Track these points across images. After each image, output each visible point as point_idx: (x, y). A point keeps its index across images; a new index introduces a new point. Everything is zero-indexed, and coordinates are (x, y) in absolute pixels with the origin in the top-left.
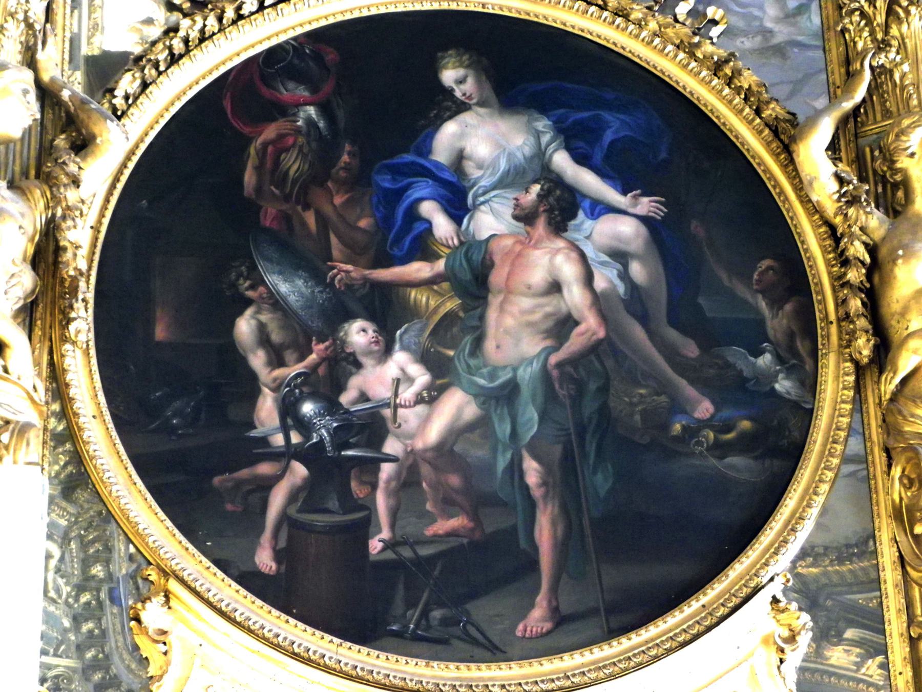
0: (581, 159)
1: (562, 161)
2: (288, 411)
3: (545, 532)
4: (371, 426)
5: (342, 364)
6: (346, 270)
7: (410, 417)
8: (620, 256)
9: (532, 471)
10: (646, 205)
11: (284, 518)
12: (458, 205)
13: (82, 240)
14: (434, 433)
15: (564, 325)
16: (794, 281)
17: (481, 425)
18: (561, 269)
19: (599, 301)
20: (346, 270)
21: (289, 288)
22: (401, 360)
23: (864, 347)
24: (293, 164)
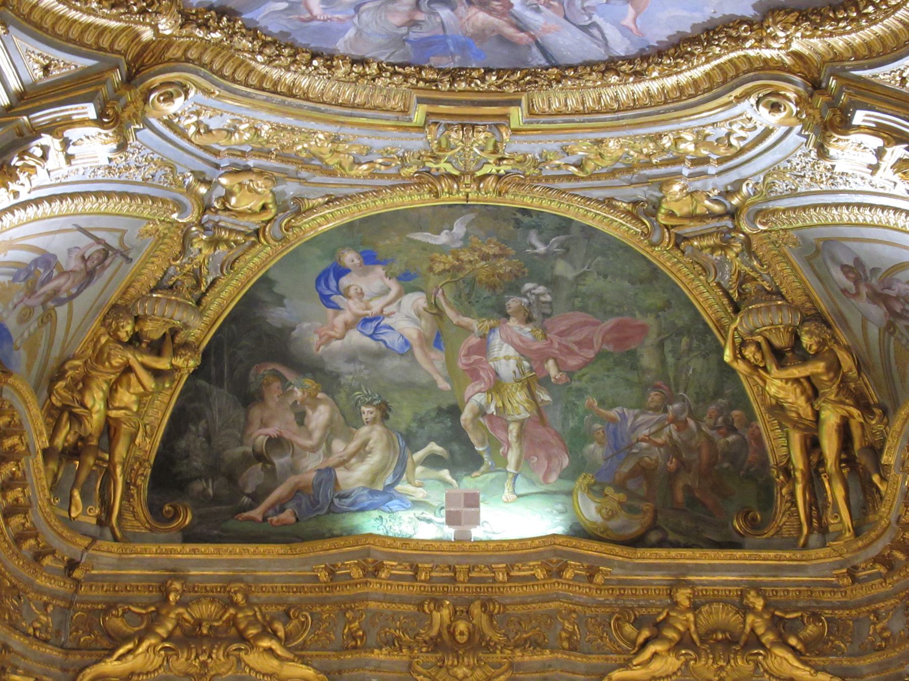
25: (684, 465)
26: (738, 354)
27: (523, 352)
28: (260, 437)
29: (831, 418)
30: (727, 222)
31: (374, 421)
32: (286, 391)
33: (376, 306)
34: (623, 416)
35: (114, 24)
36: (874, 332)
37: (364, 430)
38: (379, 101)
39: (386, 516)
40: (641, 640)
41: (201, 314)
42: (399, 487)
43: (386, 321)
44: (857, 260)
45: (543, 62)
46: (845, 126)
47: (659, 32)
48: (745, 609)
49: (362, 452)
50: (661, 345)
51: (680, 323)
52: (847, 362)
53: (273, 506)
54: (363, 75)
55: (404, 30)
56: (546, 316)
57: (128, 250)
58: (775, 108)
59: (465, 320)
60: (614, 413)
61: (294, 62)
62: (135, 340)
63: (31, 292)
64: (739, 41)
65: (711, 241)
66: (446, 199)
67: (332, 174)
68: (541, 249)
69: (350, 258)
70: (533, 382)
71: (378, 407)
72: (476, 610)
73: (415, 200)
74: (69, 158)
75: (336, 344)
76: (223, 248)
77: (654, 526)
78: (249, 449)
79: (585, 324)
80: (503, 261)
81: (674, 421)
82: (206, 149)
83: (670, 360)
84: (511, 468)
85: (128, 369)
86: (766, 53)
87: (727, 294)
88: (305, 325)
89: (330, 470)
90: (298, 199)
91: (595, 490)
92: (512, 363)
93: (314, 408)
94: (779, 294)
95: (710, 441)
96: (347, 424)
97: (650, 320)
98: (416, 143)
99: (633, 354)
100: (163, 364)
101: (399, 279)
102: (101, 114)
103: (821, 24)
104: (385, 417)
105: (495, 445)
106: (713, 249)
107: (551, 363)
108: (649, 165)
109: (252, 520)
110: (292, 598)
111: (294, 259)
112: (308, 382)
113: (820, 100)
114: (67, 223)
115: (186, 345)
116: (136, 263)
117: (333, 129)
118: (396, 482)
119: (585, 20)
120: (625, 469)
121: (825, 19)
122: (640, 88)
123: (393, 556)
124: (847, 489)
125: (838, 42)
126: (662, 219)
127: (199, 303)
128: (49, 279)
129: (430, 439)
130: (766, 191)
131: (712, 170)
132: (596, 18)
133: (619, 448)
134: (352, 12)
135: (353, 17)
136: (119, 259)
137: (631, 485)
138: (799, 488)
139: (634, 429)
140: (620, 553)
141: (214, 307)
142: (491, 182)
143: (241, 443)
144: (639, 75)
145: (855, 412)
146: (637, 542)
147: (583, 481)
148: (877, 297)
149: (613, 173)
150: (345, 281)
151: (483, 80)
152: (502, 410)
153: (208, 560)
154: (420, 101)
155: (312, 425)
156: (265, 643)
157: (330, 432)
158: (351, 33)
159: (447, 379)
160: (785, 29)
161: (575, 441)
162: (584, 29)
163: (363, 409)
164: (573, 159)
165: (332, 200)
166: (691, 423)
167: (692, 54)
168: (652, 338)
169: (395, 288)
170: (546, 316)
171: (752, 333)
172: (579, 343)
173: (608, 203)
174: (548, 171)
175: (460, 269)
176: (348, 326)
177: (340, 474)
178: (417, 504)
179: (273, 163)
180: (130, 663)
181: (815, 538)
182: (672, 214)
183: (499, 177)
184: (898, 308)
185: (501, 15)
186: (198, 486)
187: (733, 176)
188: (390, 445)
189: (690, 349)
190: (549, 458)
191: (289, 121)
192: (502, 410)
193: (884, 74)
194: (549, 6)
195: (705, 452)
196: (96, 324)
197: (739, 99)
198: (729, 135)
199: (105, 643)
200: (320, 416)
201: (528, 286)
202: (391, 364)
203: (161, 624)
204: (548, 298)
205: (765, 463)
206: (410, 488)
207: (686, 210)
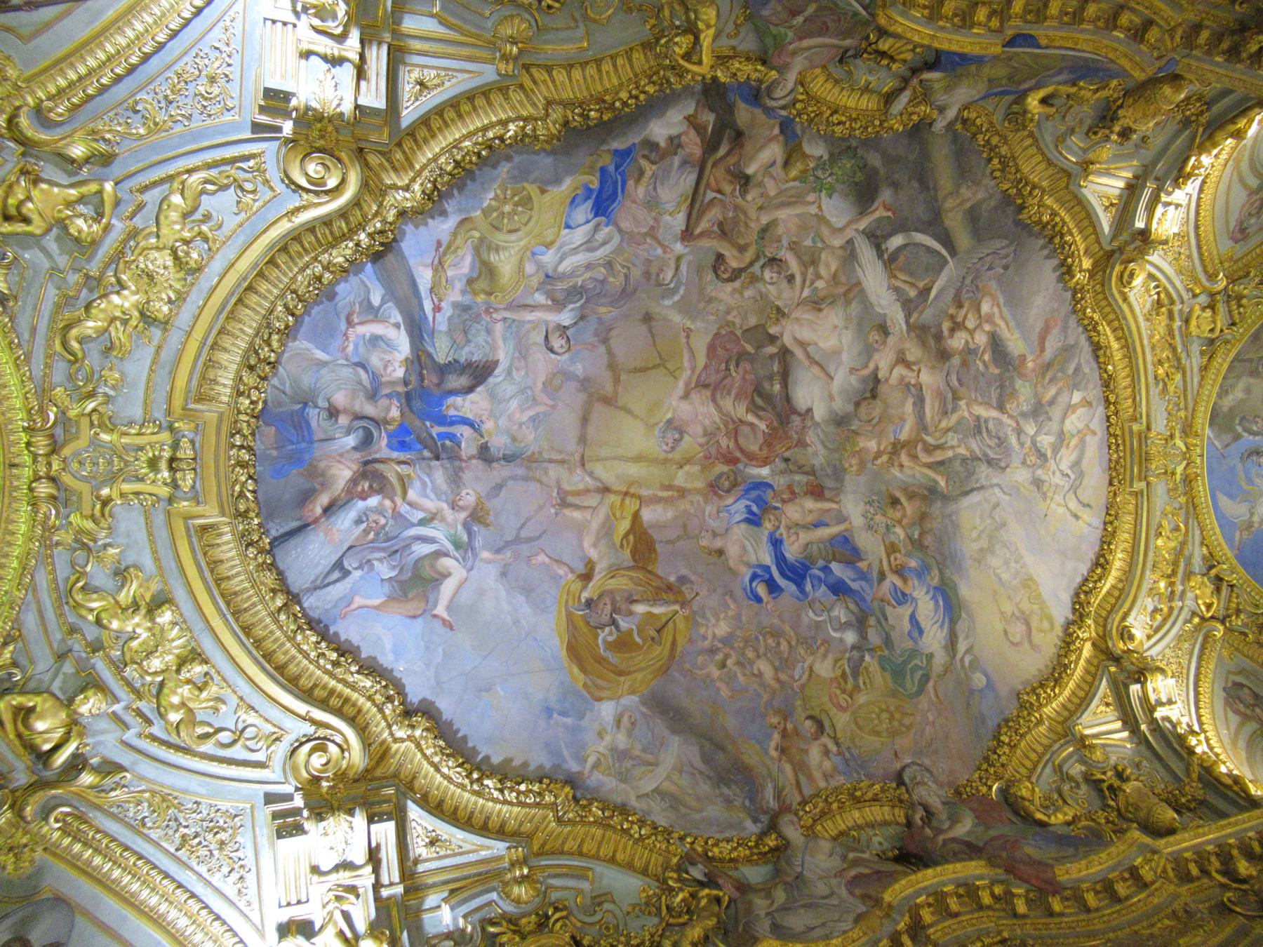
55: (322, 403)
132: (357, 574)
134: (356, 360)
135: (347, 359)
158: (320, 355)
162: (339, 565)
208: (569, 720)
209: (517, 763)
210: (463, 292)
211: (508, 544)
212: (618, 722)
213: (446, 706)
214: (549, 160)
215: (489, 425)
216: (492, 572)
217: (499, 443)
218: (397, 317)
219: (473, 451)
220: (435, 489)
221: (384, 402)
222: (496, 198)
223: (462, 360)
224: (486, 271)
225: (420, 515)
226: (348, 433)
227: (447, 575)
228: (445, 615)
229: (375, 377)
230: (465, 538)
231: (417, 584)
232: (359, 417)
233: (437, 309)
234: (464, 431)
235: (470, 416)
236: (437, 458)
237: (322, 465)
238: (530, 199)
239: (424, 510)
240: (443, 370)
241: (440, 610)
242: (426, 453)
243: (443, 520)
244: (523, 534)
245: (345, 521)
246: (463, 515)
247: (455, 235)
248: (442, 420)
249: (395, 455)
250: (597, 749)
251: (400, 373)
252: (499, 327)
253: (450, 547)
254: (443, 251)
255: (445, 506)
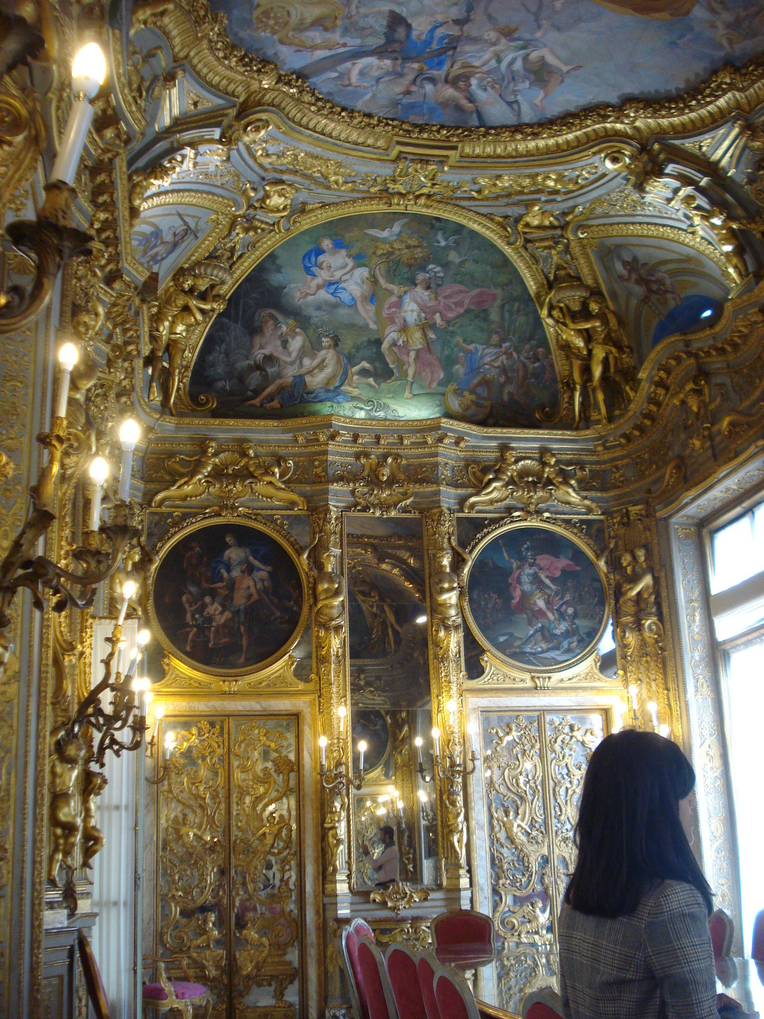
0: (255, 558)
1: (251, 559)
2: (193, 617)
3: (244, 642)
4: (210, 619)
5: (204, 606)
6: (205, 585)
7: (218, 617)
8: (262, 580)
9: (242, 628)
10: (269, 568)
11: (192, 640)
12: (229, 570)
13: (150, 581)
14: (223, 620)
15: (251, 595)
16: (299, 586)
17: (232, 619)
18: (249, 582)
19: (258, 591)
20: (205, 585)
21: (193, 589)
22: (216, 605)
23: (311, 601)
24: (194, 561)
25: (509, 380)
26: (550, 315)
27: (422, 308)
28: (259, 355)
29: (599, 353)
30: (559, 232)
31: (329, 347)
32: (277, 326)
33: (338, 275)
34: (477, 350)
35: (239, 77)
36: (634, 302)
37: (323, 352)
38: (370, 141)
39: (335, 405)
40: (486, 480)
41: (231, 275)
42: (343, 388)
43: (342, 285)
44: (635, 259)
45: (477, 123)
46: (660, 174)
47: (554, 109)
48: (544, 464)
49: (321, 366)
50: (502, 307)
51: (515, 294)
52: (613, 322)
53: (266, 398)
54: (369, 125)
56: (438, 285)
57: (198, 231)
58: (615, 160)
59: (391, 286)
60: (471, 347)
61: (331, 112)
62: (192, 290)
63: (145, 253)
64: (605, 118)
65: (546, 244)
66: (395, 209)
67: (328, 188)
68: (443, 243)
69: (327, 244)
70: (426, 326)
71: (332, 338)
72: (390, 460)
73: (376, 208)
74: (195, 164)
75: (310, 298)
76: (251, 233)
77: (491, 415)
78: (252, 363)
79: (461, 292)
80: (419, 250)
81: (505, 353)
82: (261, 166)
83: (507, 316)
84: (410, 379)
85: (186, 309)
86: (618, 126)
87: (547, 278)
88: (293, 285)
89: (301, 377)
90: (304, 204)
91: (458, 393)
92: (415, 314)
93: (293, 338)
94: (579, 279)
95: (524, 365)
96: (313, 348)
97: (499, 292)
98: (386, 170)
99: (486, 311)
100: (207, 307)
101: (354, 258)
102: (223, 135)
103: (659, 110)
104: (336, 345)
105: (401, 364)
106: (545, 248)
107: (438, 315)
108: (521, 193)
109: (254, 406)
110: (282, 451)
111: (290, 244)
112: (291, 322)
113: (645, 157)
114: (169, 209)
115: (218, 296)
116: (200, 240)
117: (341, 158)
118: (341, 385)
119: (511, 98)
120: (476, 381)
121: (663, 107)
122: (532, 145)
123: (345, 428)
124: (605, 394)
125: (665, 122)
126: (520, 227)
127: (231, 267)
128: (155, 246)
129: (363, 359)
130: (591, 214)
131: (559, 198)
132: (519, 98)
133: (473, 370)
134: (374, 82)
136: (192, 237)
137: (479, 390)
138: (577, 395)
139: (482, 357)
140: (475, 430)
141: (238, 272)
142: (422, 201)
143: (247, 358)
144: (535, 135)
145: (614, 350)
146: (482, 423)
147: (451, 387)
148: (641, 281)
149: (497, 197)
150: (321, 258)
151: (438, 132)
152: (406, 343)
153: (229, 429)
154: (399, 143)
155: (291, 349)
156: (268, 479)
157: (302, 353)
158: (368, 96)
159: (375, 323)
160: (636, 111)
161: (448, 363)
162: (509, 104)
163: (324, 339)
164: (476, 187)
165: (324, 205)
166: (515, 354)
167: (573, 124)
168: (498, 302)
169: (351, 263)
170: (438, 285)
171: (559, 302)
172: (456, 304)
173: (489, 217)
174: (459, 194)
175: (392, 253)
176: (319, 287)
177: (308, 379)
178: (354, 398)
179: (297, 179)
180: (188, 489)
181: (582, 424)
182: (527, 225)
183: (429, 196)
184: (654, 287)
185: (462, 91)
186: (220, 384)
187: (571, 203)
188: (338, 362)
189: (519, 311)
190: (432, 373)
191: (318, 151)
192: (406, 343)
193: (688, 144)
194: (493, 88)
195: (521, 373)
196: (169, 278)
197: (594, 154)
198: (578, 176)
199: (168, 478)
200: (296, 343)
201: (431, 266)
202: (342, 312)
203: (204, 467)
204: (441, 275)
205: (555, 380)
206: (350, 389)
207: (536, 223)
208: (688, 37)
209: (692, 78)
210: (334, 32)
211: (537, 20)
212: (713, 11)
213: (632, 88)
214: (235, 12)
215: (440, 18)
216: (553, 35)
217: (455, 12)
218: (348, 64)
219: (457, 28)
220: (478, 51)
221: (406, 71)
222: (265, 31)
223: (385, 30)
224: (320, 23)
225: (493, 63)
226: (423, 87)
227: (543, 58)
228: (570, 67)
229: (388, 74)
230: (520, 43)
231: (540, 74)
232: (414, 82)
233: (345, 45)
234: (439, 32)
235: (429, 27)
236: (455, 48)
237: (441, 100)
238: (264, 13)
239: (491, 59)
240: (390, 39)
241: (565, 69)
242: (450, 53)
243: (502, 51)
244: (534, 8)
245: (480, 95)
246: (503, 41)
247: (291, 44)
248: (428, 43)
249: (445, 68)
250: (720, 33)
251: (388, 62)
252: (362, 10)
253: (523, 51)
254: (302, 47)
255: (492, 49)
